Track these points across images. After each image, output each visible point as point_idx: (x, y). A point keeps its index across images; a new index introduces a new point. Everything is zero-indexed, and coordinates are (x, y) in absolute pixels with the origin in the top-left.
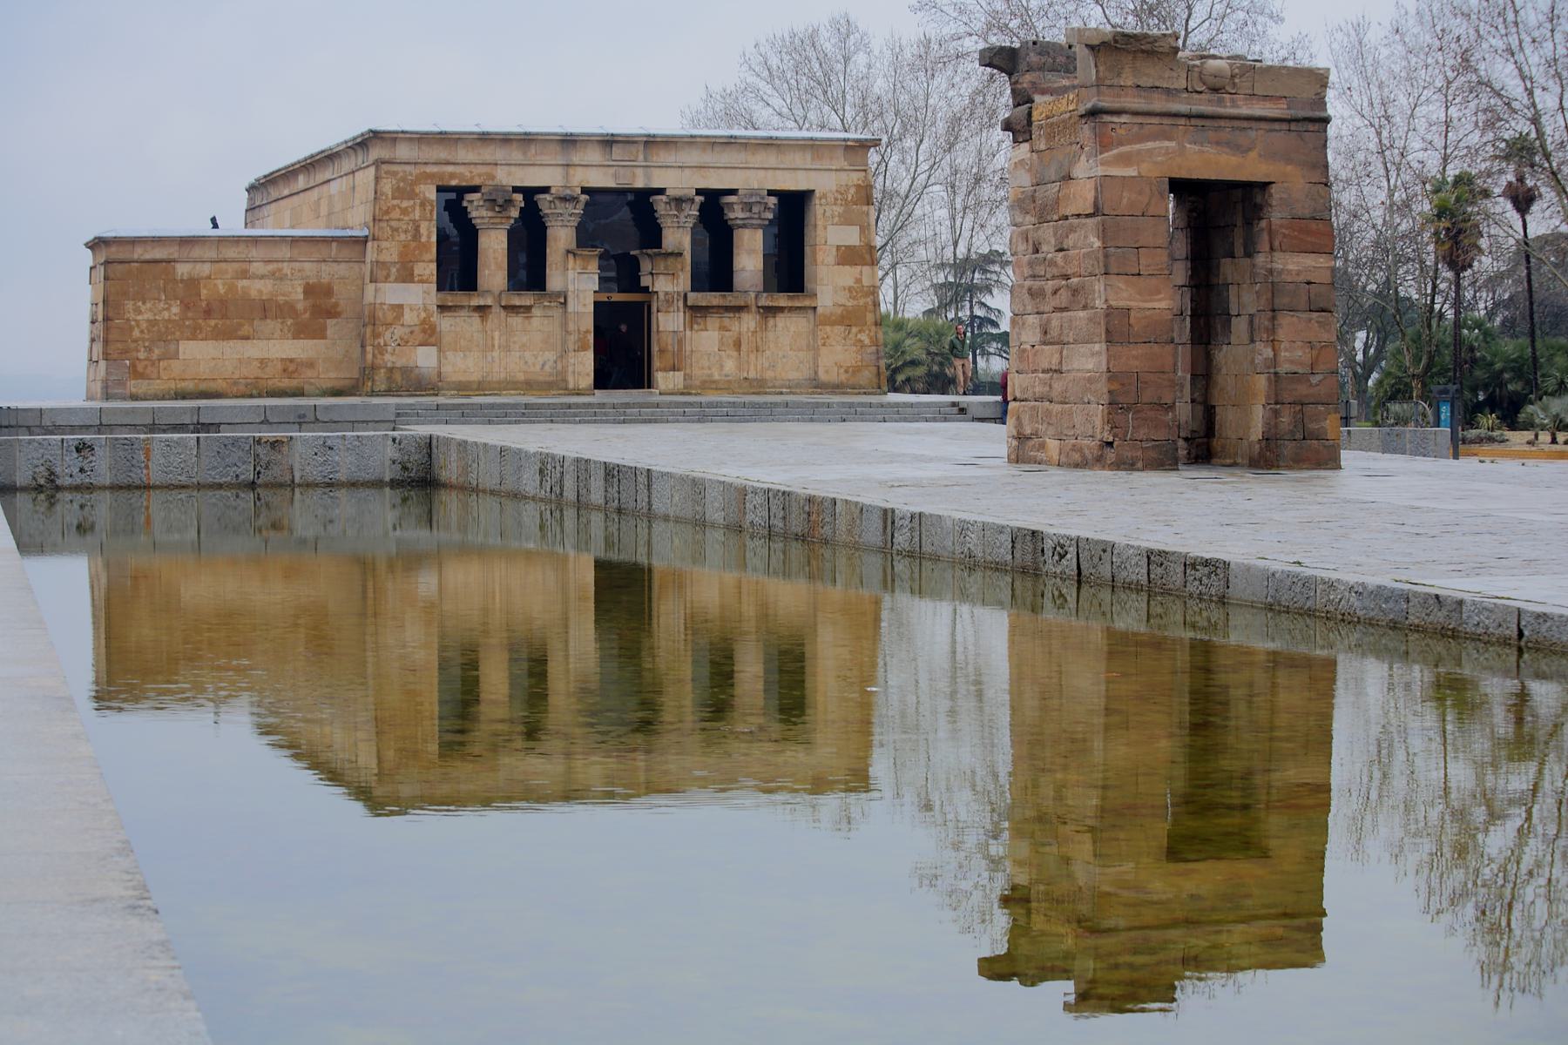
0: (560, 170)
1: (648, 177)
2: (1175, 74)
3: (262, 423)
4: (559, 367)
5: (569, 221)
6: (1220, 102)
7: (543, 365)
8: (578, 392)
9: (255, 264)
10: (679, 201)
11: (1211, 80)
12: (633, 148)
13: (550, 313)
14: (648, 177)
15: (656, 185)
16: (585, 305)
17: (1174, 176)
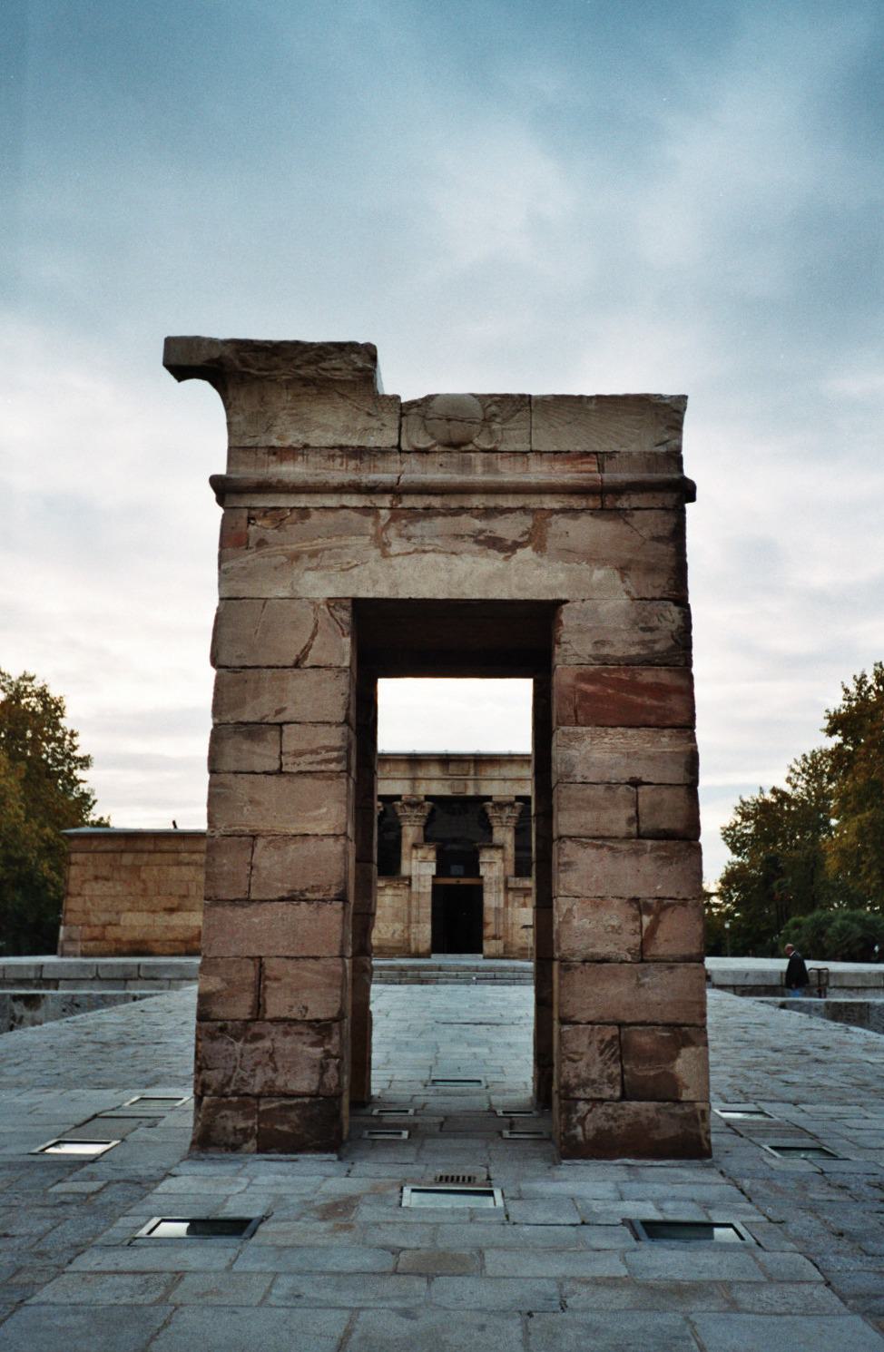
0: (407, 783)
1: (477, 787)
2: (375, 423)
3: (93, 979)
4: (406, 935)
5: (415, 821)
6: (466, 466)
7: (394, 933)
8: (418, 955)
9: (183, 854)
10: (500, 806)
11: (442, 430)
12: (466, 766)
13: (399, 892)
14: (477, 787)
15: (485, 791)
16: (424, 887)
17: (363, 594)
